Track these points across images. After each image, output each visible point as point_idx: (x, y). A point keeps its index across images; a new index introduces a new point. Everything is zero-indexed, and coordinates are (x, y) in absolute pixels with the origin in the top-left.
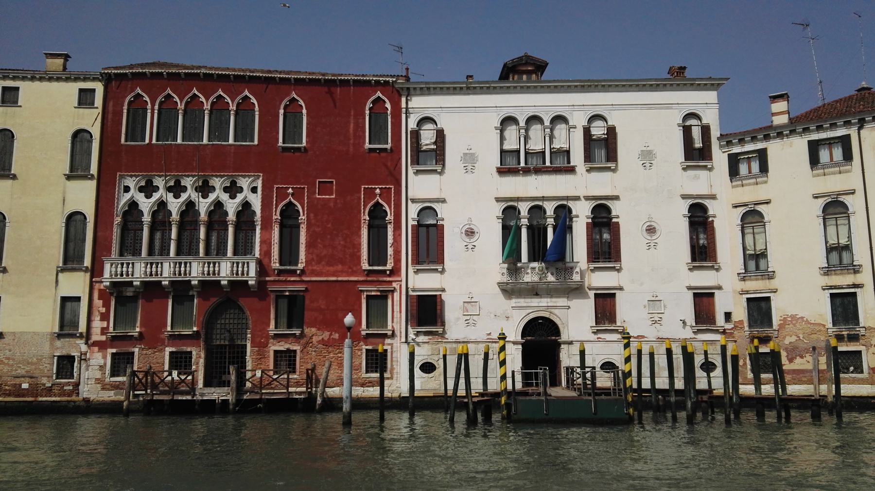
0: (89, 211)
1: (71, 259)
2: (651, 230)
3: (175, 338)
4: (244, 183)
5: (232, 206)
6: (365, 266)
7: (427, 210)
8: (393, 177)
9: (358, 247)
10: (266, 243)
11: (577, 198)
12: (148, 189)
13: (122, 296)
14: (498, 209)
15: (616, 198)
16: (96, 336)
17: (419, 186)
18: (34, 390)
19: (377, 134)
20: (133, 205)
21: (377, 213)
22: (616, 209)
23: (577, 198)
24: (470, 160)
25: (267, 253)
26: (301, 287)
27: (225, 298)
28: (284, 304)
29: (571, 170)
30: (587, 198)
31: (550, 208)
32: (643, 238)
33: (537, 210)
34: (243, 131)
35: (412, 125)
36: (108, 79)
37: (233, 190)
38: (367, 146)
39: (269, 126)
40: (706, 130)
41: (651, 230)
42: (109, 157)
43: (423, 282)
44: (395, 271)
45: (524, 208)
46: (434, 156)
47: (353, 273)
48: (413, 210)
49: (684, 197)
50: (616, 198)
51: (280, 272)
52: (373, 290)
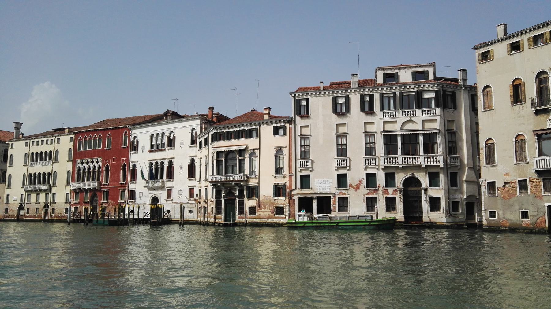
0: (71, 170)
1: (68, 183)
2: (181, 168)
3: (85, 203)
4: (99, 160)
5: (97, 166)
6: (121, 182)
7: (134, 165)
8: (128, 156)
9: (119, 177)
10: (102, 176)
11: (165, 159)
12: (82, 163)
13: (77, 192)
14: (148, 164)
15: (173, 158)
16: (72, 203)
17: (134, 157)
18: (61, 217)
19: (125, 144)
20: (79, 168)
21: (124, 166)
22: (174, 162)
23: (165, 159)
24: (143, 148)
25: (102, 180)
26: (107, 189)
27: (94, 191)
28: (105, 193)
29: (165, 150)
30: (168, 159)
31: (159, 162)
32: (179, 171)
33: (157, 163)
34: (99, 146)
35: (132, 139)
36: (75, 134)
37: (97, 162)
38: (123, 146)
39: (104, 142)
40: (196, 133)
41: (181, 168)
42: (76, 155)
43: (132, 186)
44: (126, 184)
45: (154, 162)
46: (135, 149)
47: (118, 184)
48: (131, 164)
49: (189, 157)
50: (173, 158)
51: (104, 185)
52: (121, 189)
